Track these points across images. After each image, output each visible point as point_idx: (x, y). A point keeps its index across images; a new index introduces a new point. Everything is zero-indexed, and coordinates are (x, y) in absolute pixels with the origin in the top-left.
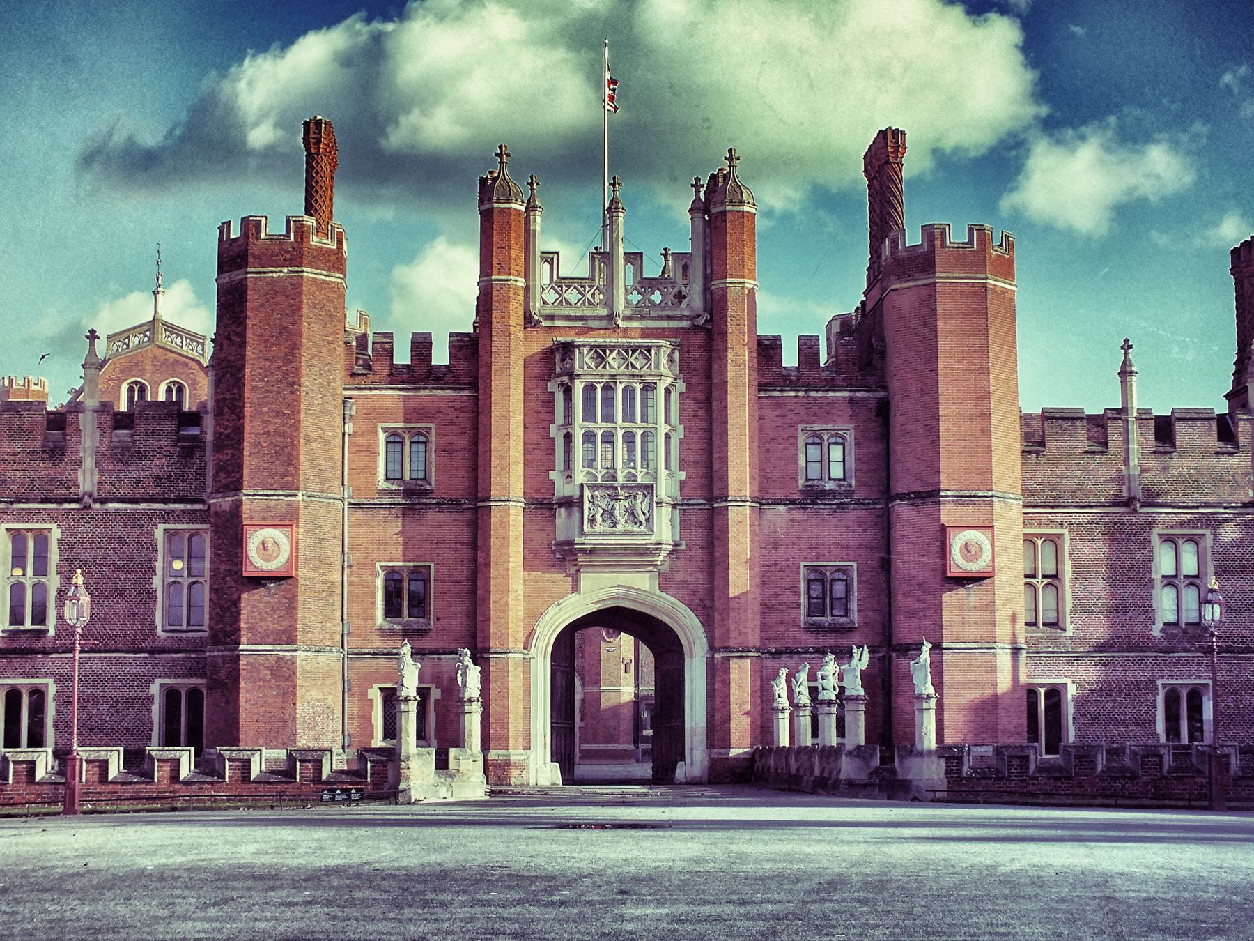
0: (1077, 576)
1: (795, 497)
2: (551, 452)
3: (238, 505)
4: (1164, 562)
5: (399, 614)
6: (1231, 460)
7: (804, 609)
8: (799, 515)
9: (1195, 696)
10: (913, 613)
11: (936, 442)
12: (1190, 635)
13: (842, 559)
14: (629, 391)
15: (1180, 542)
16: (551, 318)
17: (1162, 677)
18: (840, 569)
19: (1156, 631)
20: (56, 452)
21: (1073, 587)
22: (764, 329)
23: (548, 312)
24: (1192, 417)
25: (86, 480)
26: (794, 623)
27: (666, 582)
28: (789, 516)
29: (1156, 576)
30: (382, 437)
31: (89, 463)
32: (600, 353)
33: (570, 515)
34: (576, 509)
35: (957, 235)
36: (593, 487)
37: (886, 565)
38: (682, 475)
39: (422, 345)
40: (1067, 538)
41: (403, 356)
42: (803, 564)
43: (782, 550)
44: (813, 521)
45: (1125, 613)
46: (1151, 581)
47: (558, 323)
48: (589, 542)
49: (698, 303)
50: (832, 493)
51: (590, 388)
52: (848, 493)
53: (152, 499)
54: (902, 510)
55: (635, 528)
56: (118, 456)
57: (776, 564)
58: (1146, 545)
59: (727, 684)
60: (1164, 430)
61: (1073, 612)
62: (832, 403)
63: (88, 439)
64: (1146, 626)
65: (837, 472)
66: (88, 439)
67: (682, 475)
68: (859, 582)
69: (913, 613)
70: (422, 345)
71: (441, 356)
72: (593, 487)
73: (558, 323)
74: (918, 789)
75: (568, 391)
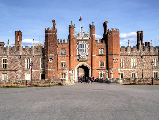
0: (124, 62)
2: (76, 51)
3: (48, 56)
4: (132, 61)
5: (63, 66)
7: (100, 65)
9: (135, 73)
10: (110, 66)
11: (112, 49)
12: (134, 68)
14: (84, 45)
16: (76, 38)
19: (131, 67)
22: (96, 39)
23: (76, 37)
24: (134, 47)
25: (33, 54)
26: (99, 67)
27: (87, 63)
29: (131, 62)
30: (61, 49)
31: (34, 52)
32: (81, 41)
33: (78, 57)
34: (79, 56)
35: (115, 29)
36: (81, 54)
38: (89, 53)
39: (64, 41)
41: (63, 42)
47: (77, 38)
48: (80, 59)
49: (90, 37)
51: (80, 45)
52: (104, 55)
53: (39, 56)
54: (109, 56)
55: (84, 58)
56: (36, 52)
58: (130, 59)
59: (93, 72)
60: (132, 49)
62: (102, 46)
63: (34, 50)
65: (103, 53)
66: (34, 50)
67: (89, 53)
69: (110, 66)
70: (64, 41)
71: (66, 42)
72: (81, 54)
73: (77, 38)
74: (119, 83)
75: (78, 45)
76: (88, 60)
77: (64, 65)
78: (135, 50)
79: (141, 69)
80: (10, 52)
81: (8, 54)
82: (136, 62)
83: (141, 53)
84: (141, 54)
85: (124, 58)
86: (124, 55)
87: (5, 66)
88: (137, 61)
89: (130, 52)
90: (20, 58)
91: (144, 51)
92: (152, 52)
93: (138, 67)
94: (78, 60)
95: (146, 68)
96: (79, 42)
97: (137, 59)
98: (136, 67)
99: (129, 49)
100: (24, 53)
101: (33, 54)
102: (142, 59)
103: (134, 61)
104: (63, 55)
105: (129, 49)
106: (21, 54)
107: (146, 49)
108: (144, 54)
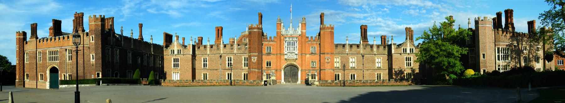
20: (232, 49)
76: (296, 59)
77: (270, 65)
78: (355, 48)
80: (210, 51)
81: (208, 53)
83: (362, 52)
85: (341, 57)
87: (205, 65)
90: (221, 56)
94: (286, 59)
96: (287, 39)
99: (347, 47)
100: (225, 51)
101: (235, 51)
104: (269, 54)
105: (347, 47)
106: (222, 52)
107: (368, 48)
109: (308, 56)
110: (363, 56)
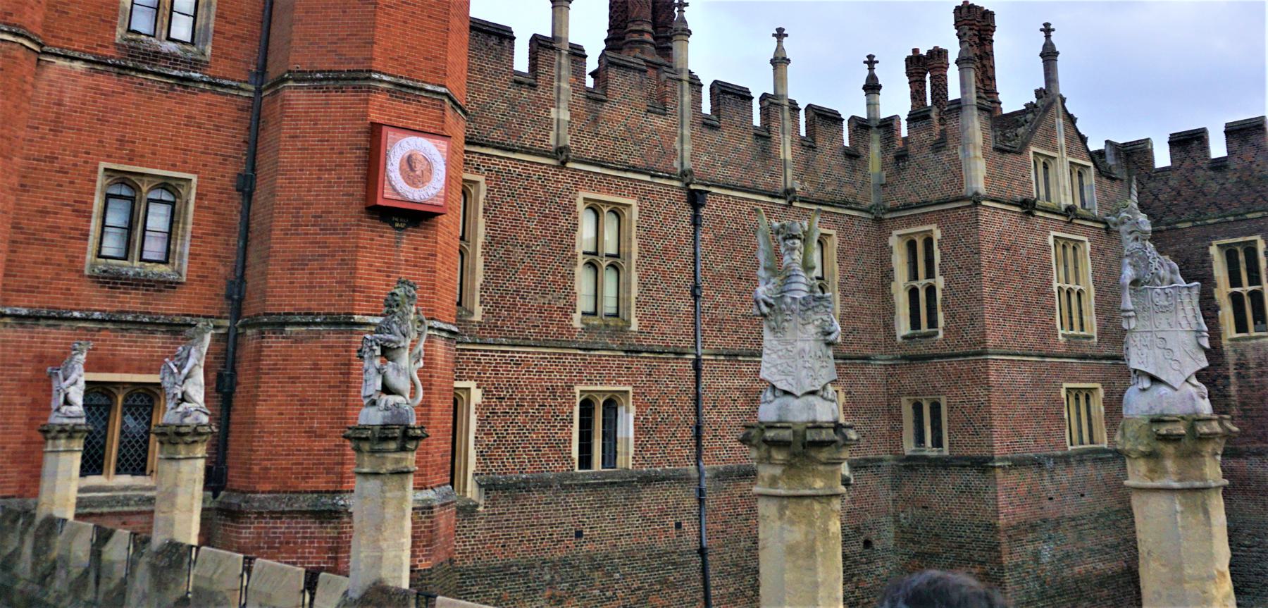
0: (492, 242)
1: (105, 52)
6: (659, 122)
8: (108, 82)
9: (611, 405)
10: (298, 263)
13: (173, 167)
15: (605, 210)
17: (581, 381)
18: (165, 184)
21: (486, 254)
28: (89, 81)
37: (246, 186)
40: (483, 187)
42: (103, 165)
43: (70, 136)
44: (134, 97)
45: (544, 295)
46: (574, 256)
50: (168, 57)
57: (52, 159)
58: (570, 209)
61: (484, 288)
64: (566, 315)
68: (198, 207)
79: (679, 354)
82: (635, 256)
83: (687, 151)
84: (688, 165)
85: (496, 178)
86: (496, 135)
88: (643, 245)
89: (565, 116)
91: (716, 137)
92: (789, 157)
93: (649, 323)
95: (732, 344)
97: (645, 214)
98: (635, 326)
102: (696, 221)
103: (610, 246)
108: (719, 173)
109: (66, 75)
110: (695, 200)
